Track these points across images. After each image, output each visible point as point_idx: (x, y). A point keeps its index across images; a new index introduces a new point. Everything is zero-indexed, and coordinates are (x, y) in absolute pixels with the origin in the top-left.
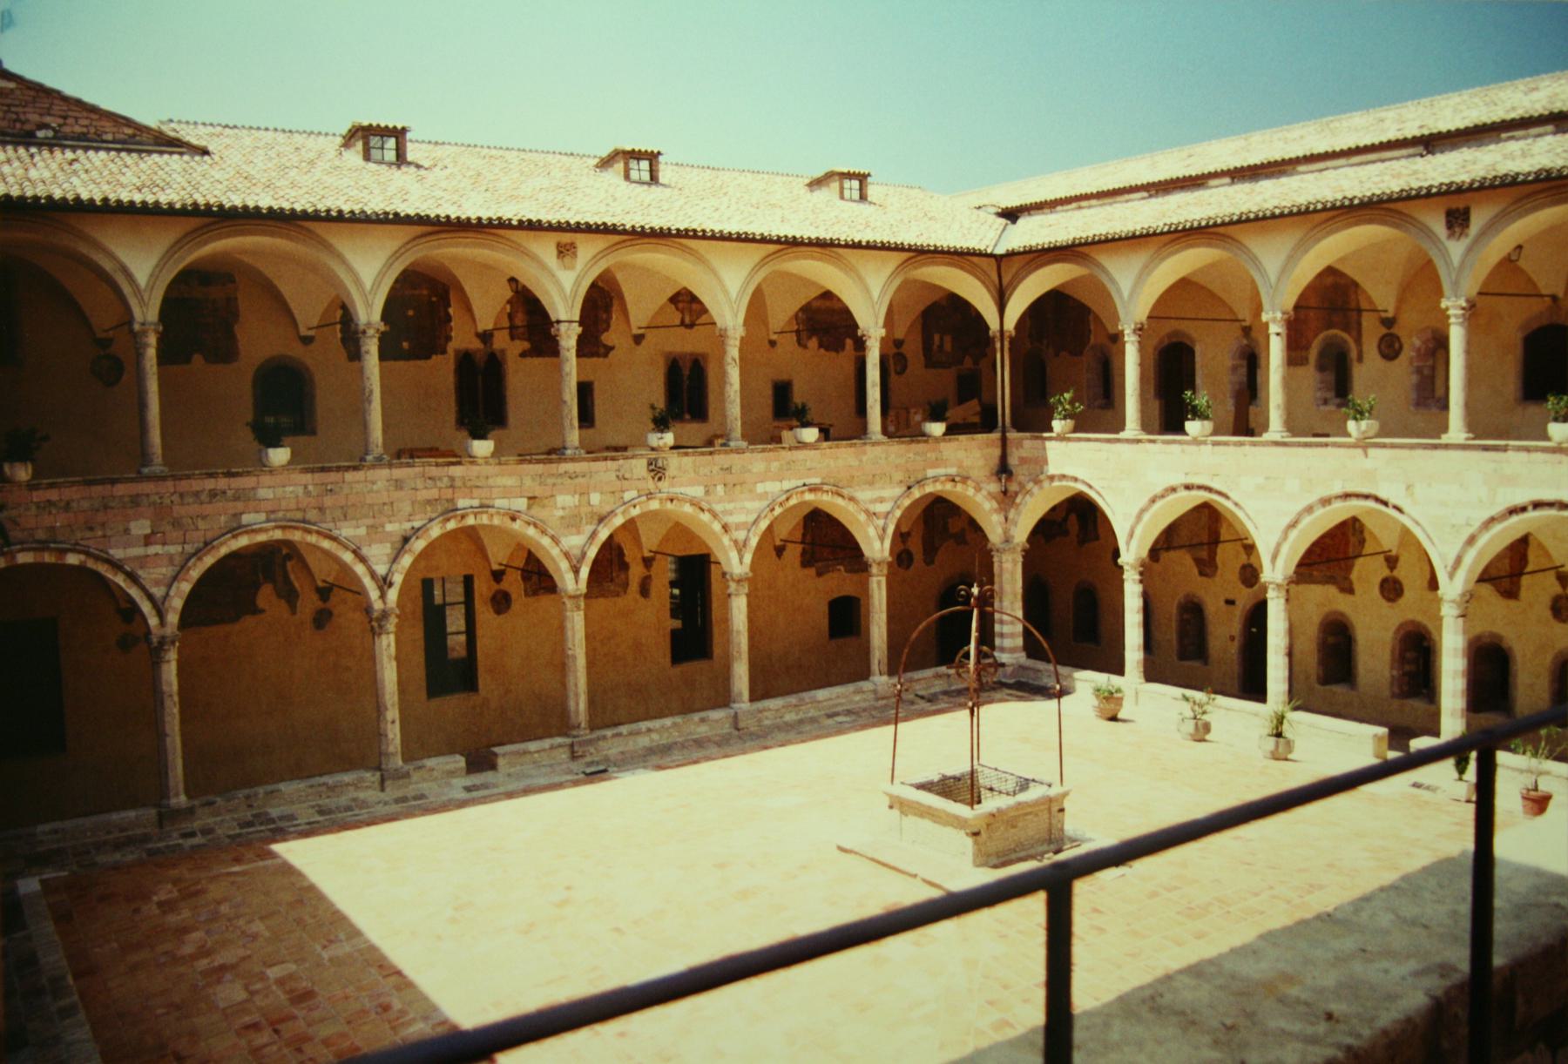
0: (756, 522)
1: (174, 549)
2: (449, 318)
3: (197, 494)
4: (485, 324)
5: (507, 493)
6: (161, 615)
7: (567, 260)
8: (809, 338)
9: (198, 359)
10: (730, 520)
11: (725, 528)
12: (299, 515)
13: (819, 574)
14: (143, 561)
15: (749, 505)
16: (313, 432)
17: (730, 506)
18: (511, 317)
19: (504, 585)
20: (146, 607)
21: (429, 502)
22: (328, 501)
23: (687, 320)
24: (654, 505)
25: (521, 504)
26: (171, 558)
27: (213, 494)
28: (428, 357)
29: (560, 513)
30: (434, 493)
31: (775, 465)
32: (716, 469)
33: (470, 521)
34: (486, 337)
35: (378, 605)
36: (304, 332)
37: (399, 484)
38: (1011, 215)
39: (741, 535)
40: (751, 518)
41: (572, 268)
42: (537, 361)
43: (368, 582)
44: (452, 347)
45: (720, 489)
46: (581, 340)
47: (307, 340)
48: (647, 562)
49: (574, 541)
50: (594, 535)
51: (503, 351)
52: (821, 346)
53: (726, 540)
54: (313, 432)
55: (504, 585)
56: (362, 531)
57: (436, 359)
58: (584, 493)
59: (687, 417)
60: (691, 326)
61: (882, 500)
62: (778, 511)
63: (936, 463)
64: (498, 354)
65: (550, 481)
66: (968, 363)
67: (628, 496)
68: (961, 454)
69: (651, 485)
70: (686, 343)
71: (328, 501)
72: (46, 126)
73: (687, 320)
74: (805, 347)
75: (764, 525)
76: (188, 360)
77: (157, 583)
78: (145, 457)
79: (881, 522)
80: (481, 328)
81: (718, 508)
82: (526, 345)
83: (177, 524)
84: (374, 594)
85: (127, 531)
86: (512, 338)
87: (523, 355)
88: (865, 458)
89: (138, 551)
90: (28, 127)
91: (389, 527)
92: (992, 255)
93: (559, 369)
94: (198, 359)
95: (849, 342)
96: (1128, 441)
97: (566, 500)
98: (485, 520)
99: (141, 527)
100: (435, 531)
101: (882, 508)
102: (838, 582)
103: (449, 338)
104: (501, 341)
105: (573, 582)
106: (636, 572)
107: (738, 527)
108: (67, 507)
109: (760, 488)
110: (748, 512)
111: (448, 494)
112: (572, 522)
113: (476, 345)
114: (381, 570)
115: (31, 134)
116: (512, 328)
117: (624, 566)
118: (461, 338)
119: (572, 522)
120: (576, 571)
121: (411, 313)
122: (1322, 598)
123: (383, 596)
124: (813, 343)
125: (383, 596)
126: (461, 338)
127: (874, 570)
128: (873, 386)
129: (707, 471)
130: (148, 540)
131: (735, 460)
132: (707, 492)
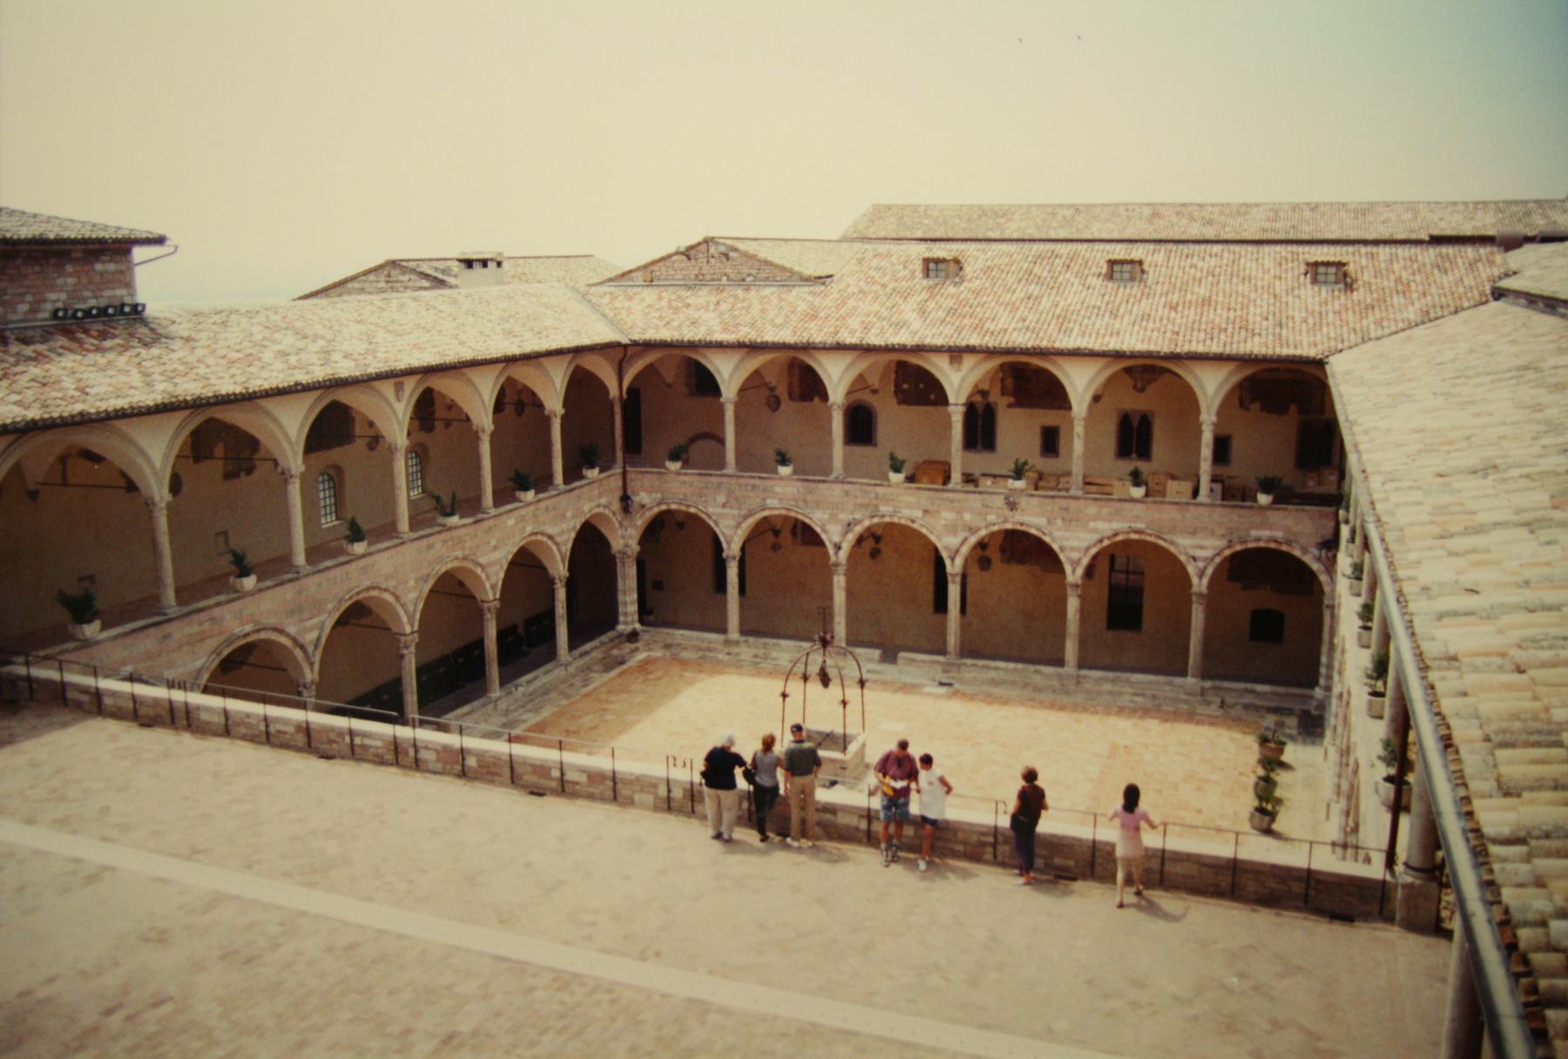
0: (1088, 549)
1: (736, 512)
3: (746, 485)
5: (909, 506)
6: (729, 543)
7: (956, 365)
8: (1251, 402)
9: (817, 399)
10: (1066, 543)
11: (1062, 549)
12: (793, 503)
14: (721, 515)
15: (1084, 535)
16: (875, 445)
17: (1067, 534)
18: (1002, 380)
19: (987, 553)
21: (862, 505)
22: (809, 498)
23: (1139, 385)
25: (918, 514)
26: (734, 517)
27: (754, 487)
29: (943, 522)
30: (865, 500)
31: (1105, 511)
32: (1056, 508)
33: (887, 519)
35: (833, 559)
37: (847, 493)
39: (1075, 555)
40: (1084, 545)
41: (959, 370)
42: (1018, 411)
43: (828, 544)
45: (1059, 522)
47: (875, 392)
49: (954, 541)
50: (965, 541)
51: (996, 404)
52: (1263, 409)
54: (875, 445)
55: (987, 553)
56: (826, 516)
58: (960, 512)
59: (1134, 456)
61: (1202, 547)
62: (1106, 543)
63: (1261, 526)
64: (993, 405)
65: (937, 502)
67: (992, 518)
68: (1290, 522)
69: (1007, 512)
71: (809, 498)
72: (749, 275)
73: (1139, 385)
74: (1247, 409)
75: (1094, 551)
76: (812, 400)
77: (727, 527)
78: (721, 464)
79: (1201, 564)
82: (1012, 400)
83: (737, 499)
84: (831, 551)
85: (715, 500)
86: (1003, 394)
87: (1010, 406)
88: (1188, 515)
89: (719, 510)
90: (743, 276)
94: (817, 399)
95: (1293, 408)
97: (947, 515)
99: (721, 499)
100: (867, 523)
101: (1199, 553)
104: (995, 397)
107: (1073, 549)
108: (691, 485)
109: (1092, 525)
111: (875, 502)
112: (952, 529)
114: (836, 539)
115: (743, 280)
119: (952, 529)
120: (953, 559)
123: (836, 554)
124: (1256, 406)
125: (836, 554)
128: (1206, 459)
129: (1049, 508)
130: (724, 506)
131: (1073, 504)
132: (1049, 523)
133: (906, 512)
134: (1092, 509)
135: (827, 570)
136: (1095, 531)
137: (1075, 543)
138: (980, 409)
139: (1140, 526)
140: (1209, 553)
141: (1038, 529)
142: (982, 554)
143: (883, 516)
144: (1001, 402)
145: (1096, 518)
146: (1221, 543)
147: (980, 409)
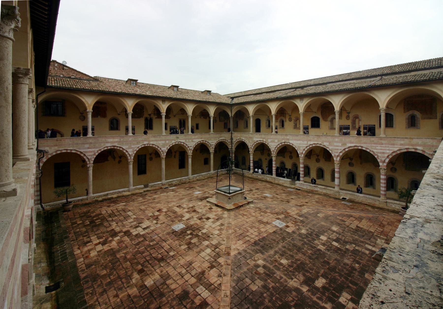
2: (144, 112)
4: (150, 113)
5: (152, 141)
10: (189, 145)
11: (188, 147)
13: (203, 154)
15: (192, 143)
17: (189, 143)
18: (154, 112)
20: (87, 160)
24: (177, 143)
28: (140, 118)
34: (150, 115)
36: (118, 113)
38: (233, 98)
39: (191, 148)
40: (193, 145)
44: (144, 117)
46: (166, 116)
48: (175, 152)
53: (188, 149)
57: (141, 118)
60: (183, 114)
66: (226, 121)
70: (182, 117)
80: (149, 113)
81: (187, 143)
87: (156, 118)
91: (133, 146)
92: (230, 104)
93: (162, 120)
96: (251, 134)
98: (149, 145)
102: (205, 156)
103: (143, 115)
104: (152, 116)
105: (163, 155)
106: (174, 154)
107: (191, 146)
109: (194, 140)
110: (192, 144)
112: (164, 146)
113: (148, 116)
116: (154, 113)
117: (172, 153)
118: (146, 115)
121: (137, 110)
122: (281, 159)
124: (202, 117)
126: (146, 115)
127: (211, 154)
132: (185, 141)
133: (151, 143)
134: (193, 137)
135: (128, 164)
136: (194, 142)
137: (191, 145)
138: (149, 119)
139: (203, 139)
140: (214, 144)
141: (184, 143)
142: (170, 152)
143: (145, 145)
144: (154, 117)
145: (195, 139)
146: (216, 141)
147: (149, 119)
